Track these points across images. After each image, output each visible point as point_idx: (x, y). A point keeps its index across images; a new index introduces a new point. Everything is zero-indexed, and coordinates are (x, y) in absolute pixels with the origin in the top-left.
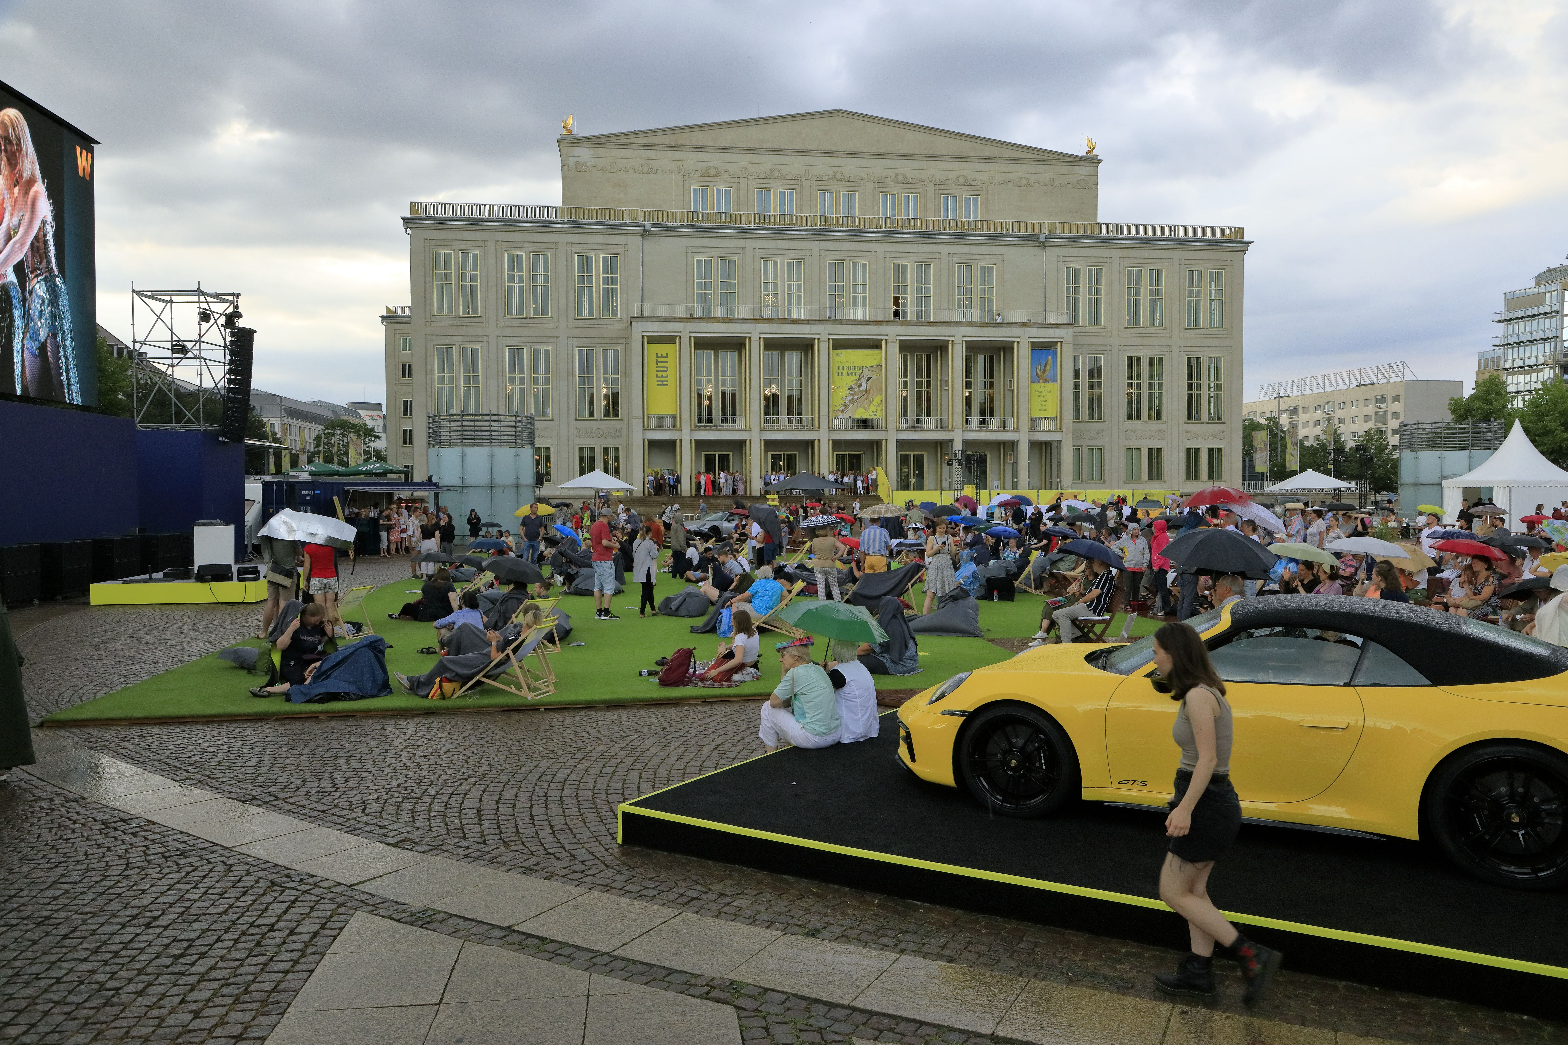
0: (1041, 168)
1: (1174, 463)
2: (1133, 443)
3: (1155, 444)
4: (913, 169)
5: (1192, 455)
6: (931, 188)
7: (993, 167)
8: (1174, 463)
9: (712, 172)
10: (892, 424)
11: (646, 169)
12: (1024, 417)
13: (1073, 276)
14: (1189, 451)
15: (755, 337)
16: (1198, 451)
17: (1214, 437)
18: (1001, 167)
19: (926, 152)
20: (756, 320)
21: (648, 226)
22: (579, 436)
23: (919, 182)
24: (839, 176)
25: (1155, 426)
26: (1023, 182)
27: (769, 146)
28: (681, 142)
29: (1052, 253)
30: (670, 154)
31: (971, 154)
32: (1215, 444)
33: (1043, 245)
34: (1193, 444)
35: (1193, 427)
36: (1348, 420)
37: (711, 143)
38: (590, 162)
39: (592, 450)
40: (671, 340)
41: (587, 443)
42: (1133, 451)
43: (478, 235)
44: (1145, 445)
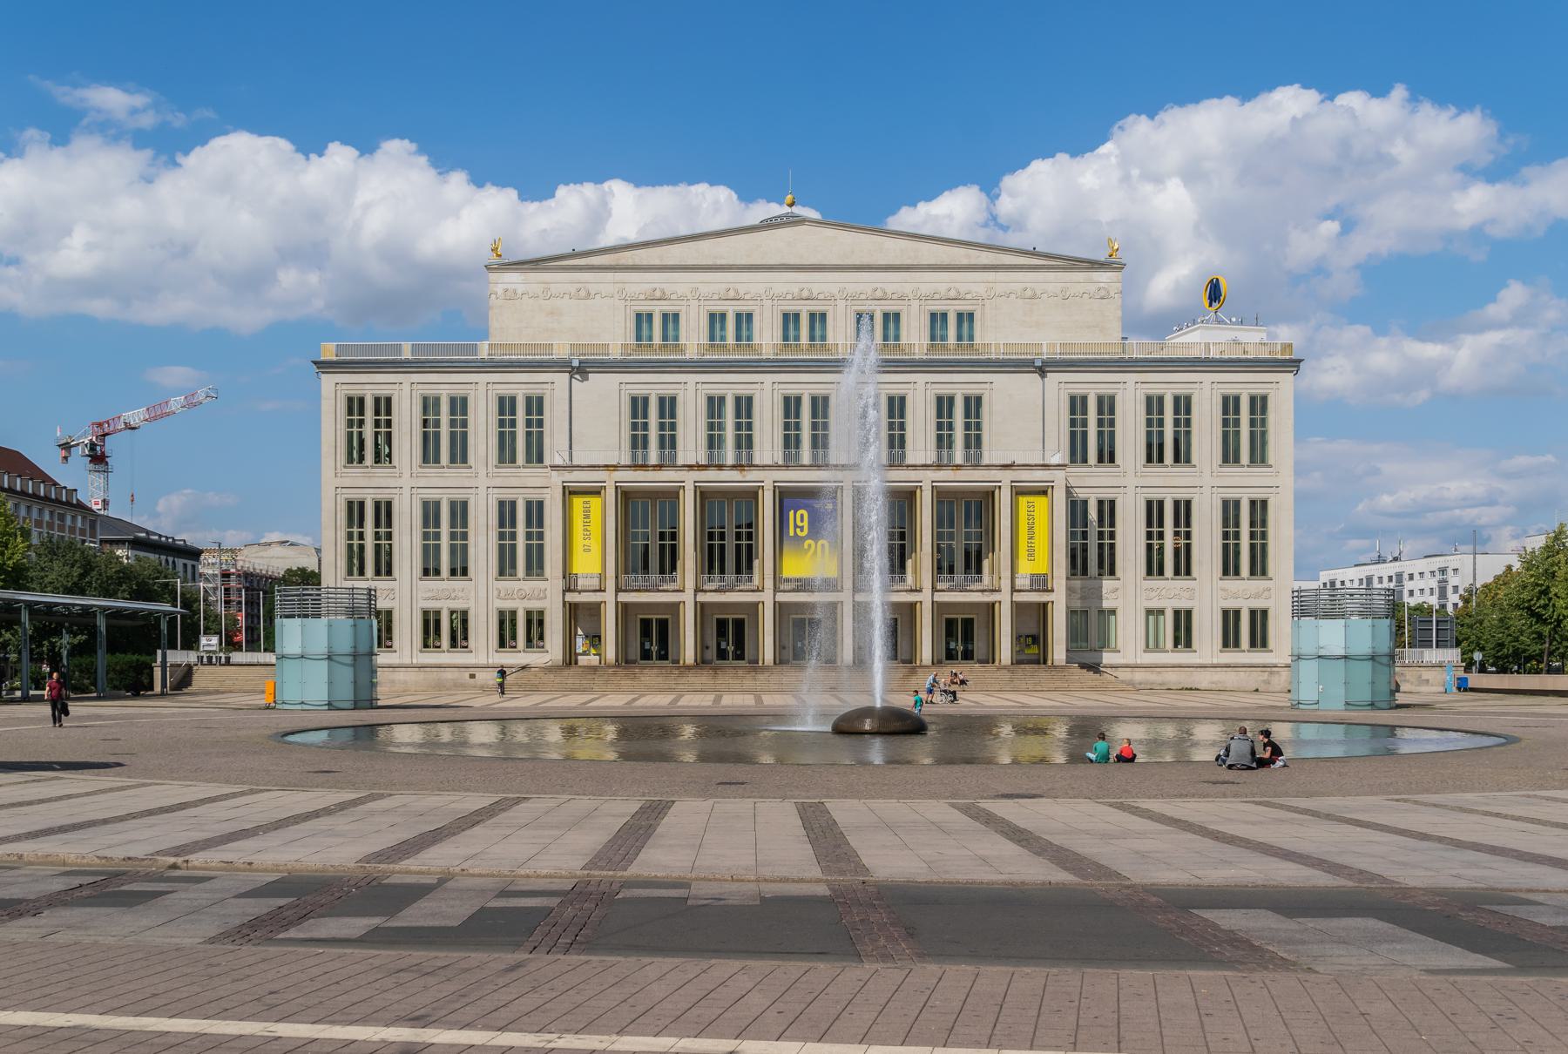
0: (1051, 276)
1: (1207, 629)
2: (1154, 604)
3: (1183, 604)
5: (1230, 618)
6: (915, 304)
7: (991, 276)
8: (1207, 629)
9: (658, 294)
10: (848, 584)
11: (583, 293)
13: (1077, 405)
14: (1225, 613)
16: (1237, 613)
17: (1257, 596)
18: (1001, 276)
19: (909, 262)
20: (690, 467)
21: (576, 363)
22: (499, 597)
25: (1182, 583)
26: (1029, 293)
27: (723, 262)
28: (622, 262)
29: (1053, 378)
30: (609, 276)
31: (965, 262)
32: (1258, 604)
33: (1042, 371)
34: (1231, 604)
35: (1232, 584)
36: (1417, 576)
37: (657, 262)
38: (520, 289)
40: (596, 492)
41: (508, 605)
44: (1169, 605)
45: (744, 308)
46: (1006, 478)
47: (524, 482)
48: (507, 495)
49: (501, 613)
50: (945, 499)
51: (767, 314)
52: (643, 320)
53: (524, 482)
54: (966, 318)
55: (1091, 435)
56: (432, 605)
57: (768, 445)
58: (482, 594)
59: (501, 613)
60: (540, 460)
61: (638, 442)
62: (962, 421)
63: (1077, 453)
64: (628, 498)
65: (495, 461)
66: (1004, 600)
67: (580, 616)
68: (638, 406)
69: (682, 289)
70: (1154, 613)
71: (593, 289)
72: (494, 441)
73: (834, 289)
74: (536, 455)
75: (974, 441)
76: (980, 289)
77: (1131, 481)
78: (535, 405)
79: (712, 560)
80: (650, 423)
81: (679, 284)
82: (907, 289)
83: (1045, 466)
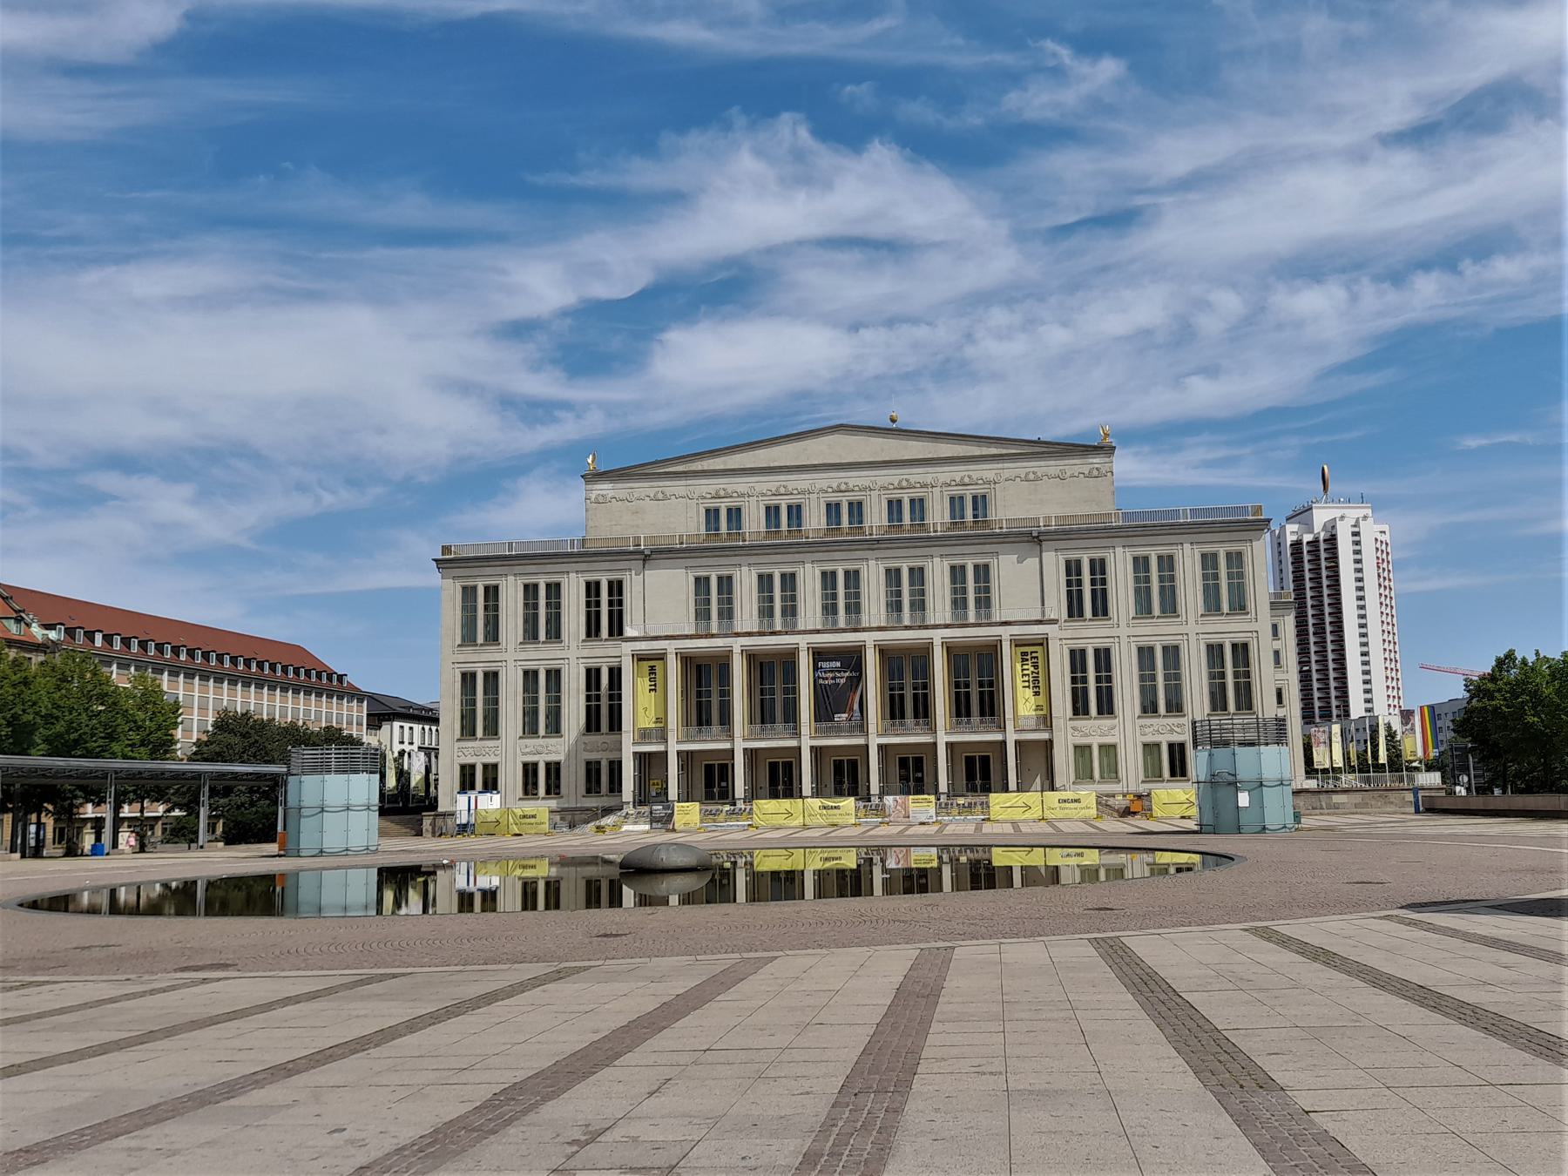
2: (1150, 739)
4: (917, 475)
12: (1009, 715)
13: (1073, 568)
15: (737, 650)
23: (924, 486)
24: (843, 487)
26: (1031, 476)
39: (599, 763)
41: (593, 756)
42: (1151, 749)
43: (499, 570)
44: (1164, 740)
45: (794, 500)
46: (1006, 633)
47: (604, 652)
48: (593, 663)
49: (588, 763)
50: (958, 656)
51: (814, 504)
52: (712, 515)
53: (604, 652)
54: (980, 502)
55: (1086, 595)
56: (530, 759)
57: (747, 612)
58: (510, 750)
59: (588, 763)
60: (621, 632)
61: (702, 614)
62: (973, 589)
63: (1075, 610)
64: (687, 660)
65: (583, 636)
66: (1011, 738)
67: (650, 764)
68: (701, 584)
69: (742, 488)
70: (1151, 749)
71: (668, 491)
72: (583, 619)
73: (865, 482)
74: (617, 629)
75: (984, 602)
76: (990, 475)
77: (1123, 631)
78: (616, 588)
79: (763, 714)
80: (713, 599)
81: (740, 484)
82: (929, 479)
83: (1040, 622)
